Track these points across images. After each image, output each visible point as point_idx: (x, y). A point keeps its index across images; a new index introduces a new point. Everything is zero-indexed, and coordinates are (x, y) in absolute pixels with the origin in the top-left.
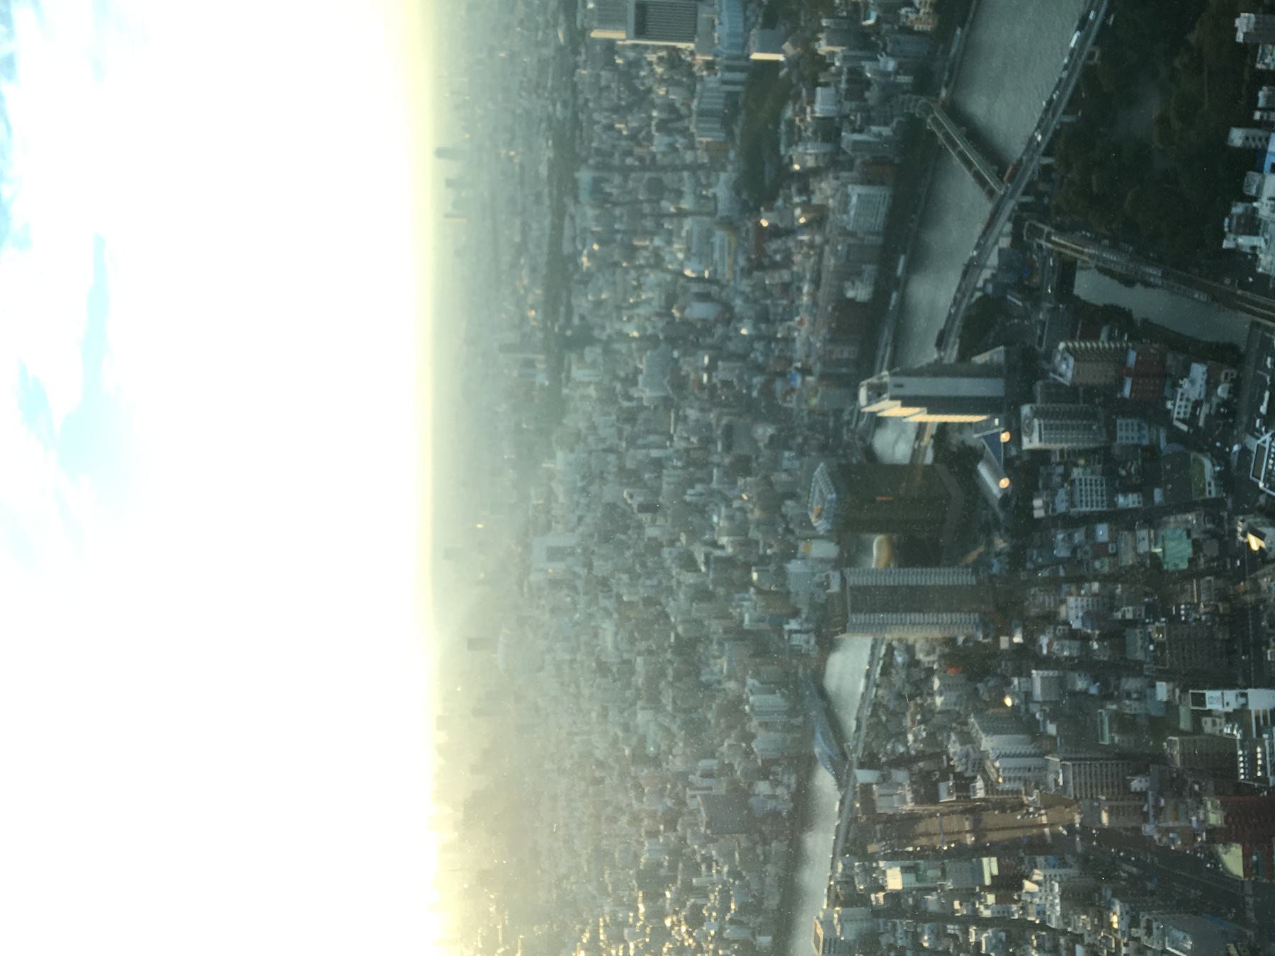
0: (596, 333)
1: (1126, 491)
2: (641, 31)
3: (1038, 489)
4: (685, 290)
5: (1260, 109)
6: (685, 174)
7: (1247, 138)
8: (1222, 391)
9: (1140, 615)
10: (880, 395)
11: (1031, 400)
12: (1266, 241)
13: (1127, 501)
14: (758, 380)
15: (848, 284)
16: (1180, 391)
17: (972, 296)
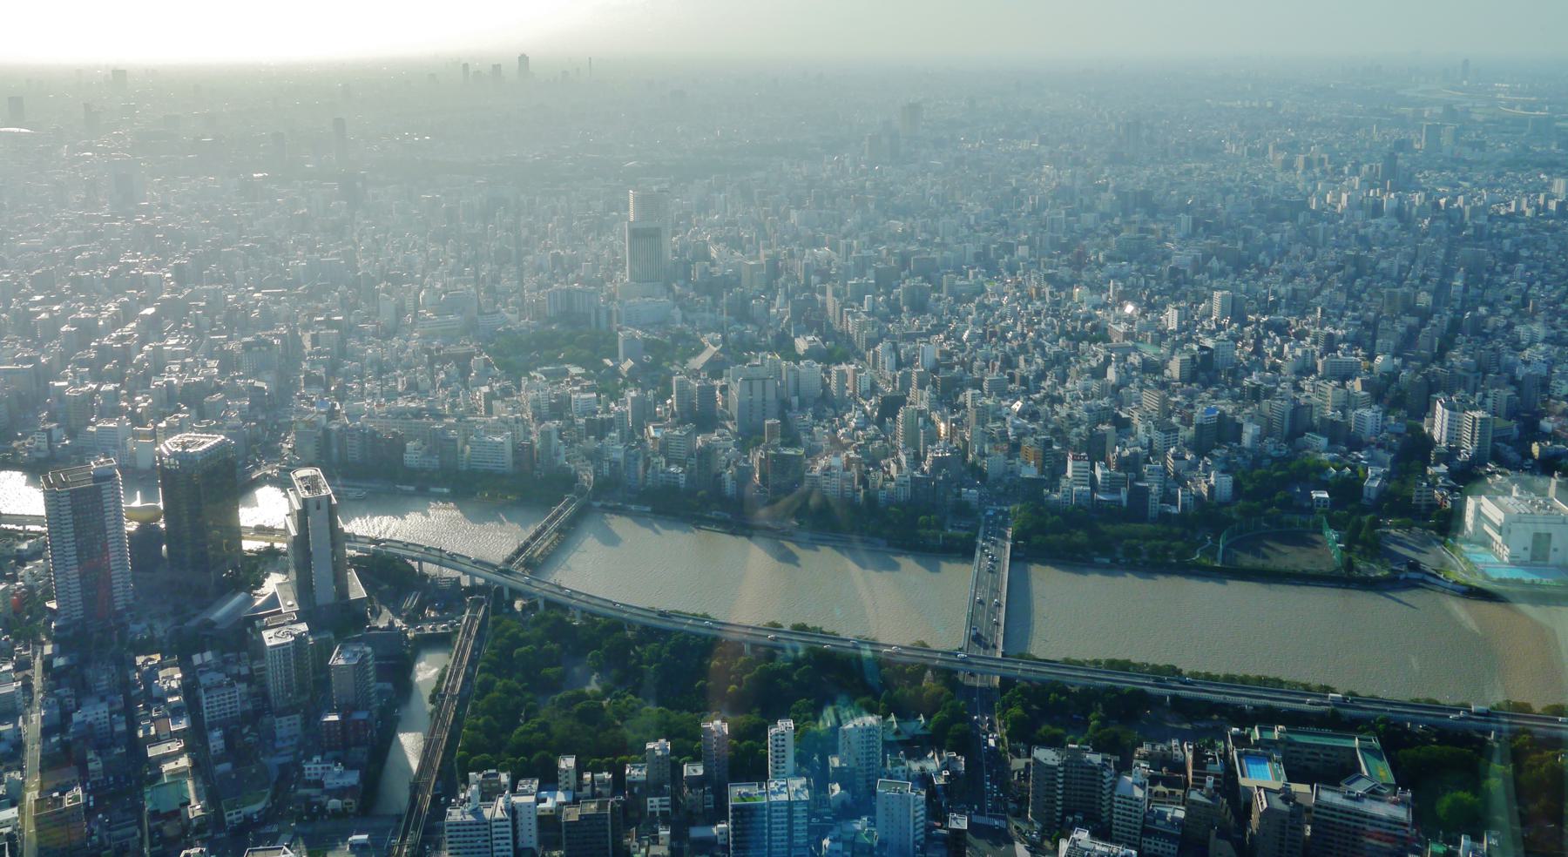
1: (228, 738)
3: (224, 653)
7: (567, 771)
8: (334, 803)
9: (93, 776)
13: (216, 740)
16: (332, 765)
17: (414, 559)
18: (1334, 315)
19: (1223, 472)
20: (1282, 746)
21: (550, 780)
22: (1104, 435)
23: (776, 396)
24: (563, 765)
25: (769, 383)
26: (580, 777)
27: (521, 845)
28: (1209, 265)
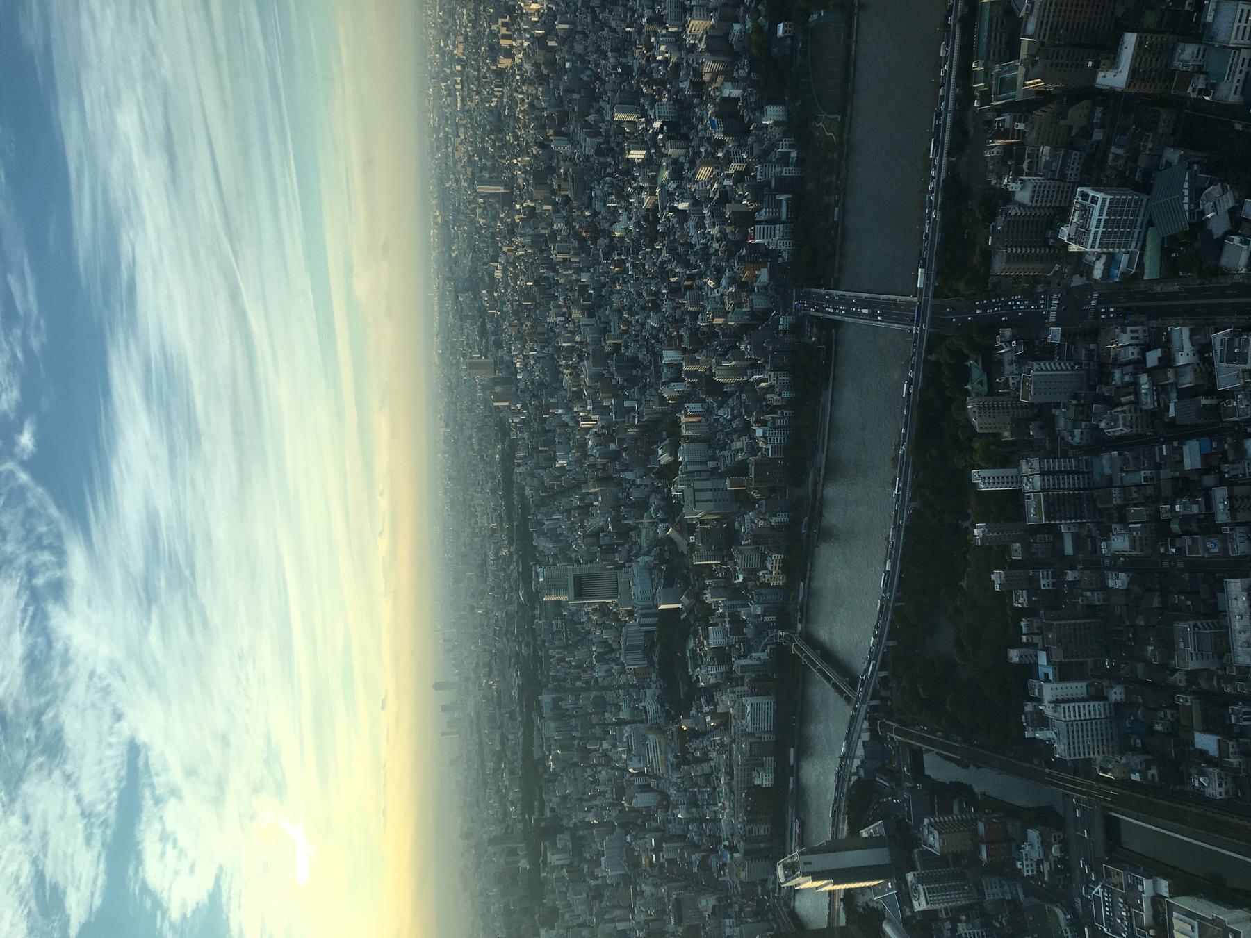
0: (565, 822)
2: (579, 594)
4: (631, 784)
5: (1024, 635)
6: (621, 692)
7: (1021, 656)
10: (794, 873)
11: (913, 869)
12: (1056, 733)
14: (696, 857)
15: (754, 774)
17: (850, 780)
18: (632, 16)
19: (762, 114)
20: (989, 64)
21: (1029, 670)
22: (733, 213)
23: (707, 480)
24: (1016, 660)
25: (698, 485)
26: (1026, 645)
27: (1085, 695)
28: (592, 123)
